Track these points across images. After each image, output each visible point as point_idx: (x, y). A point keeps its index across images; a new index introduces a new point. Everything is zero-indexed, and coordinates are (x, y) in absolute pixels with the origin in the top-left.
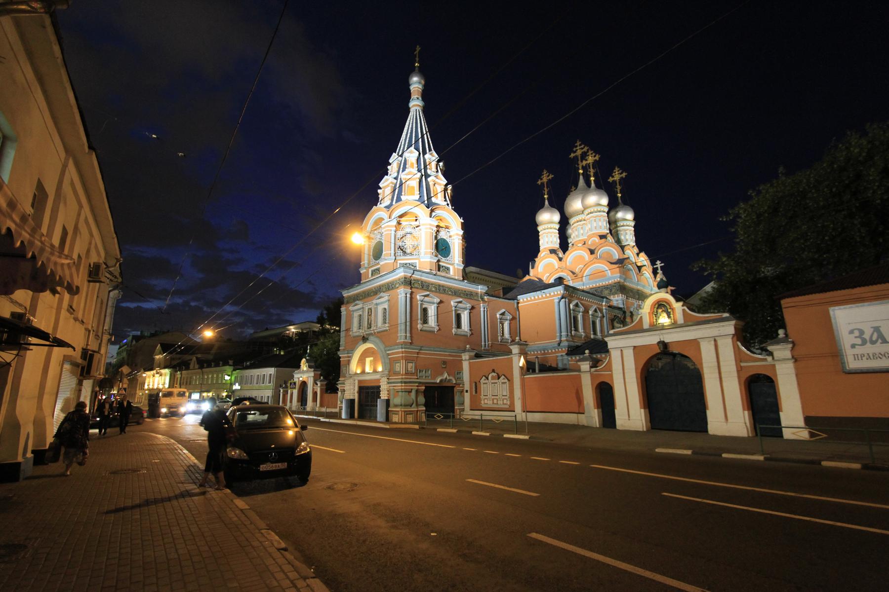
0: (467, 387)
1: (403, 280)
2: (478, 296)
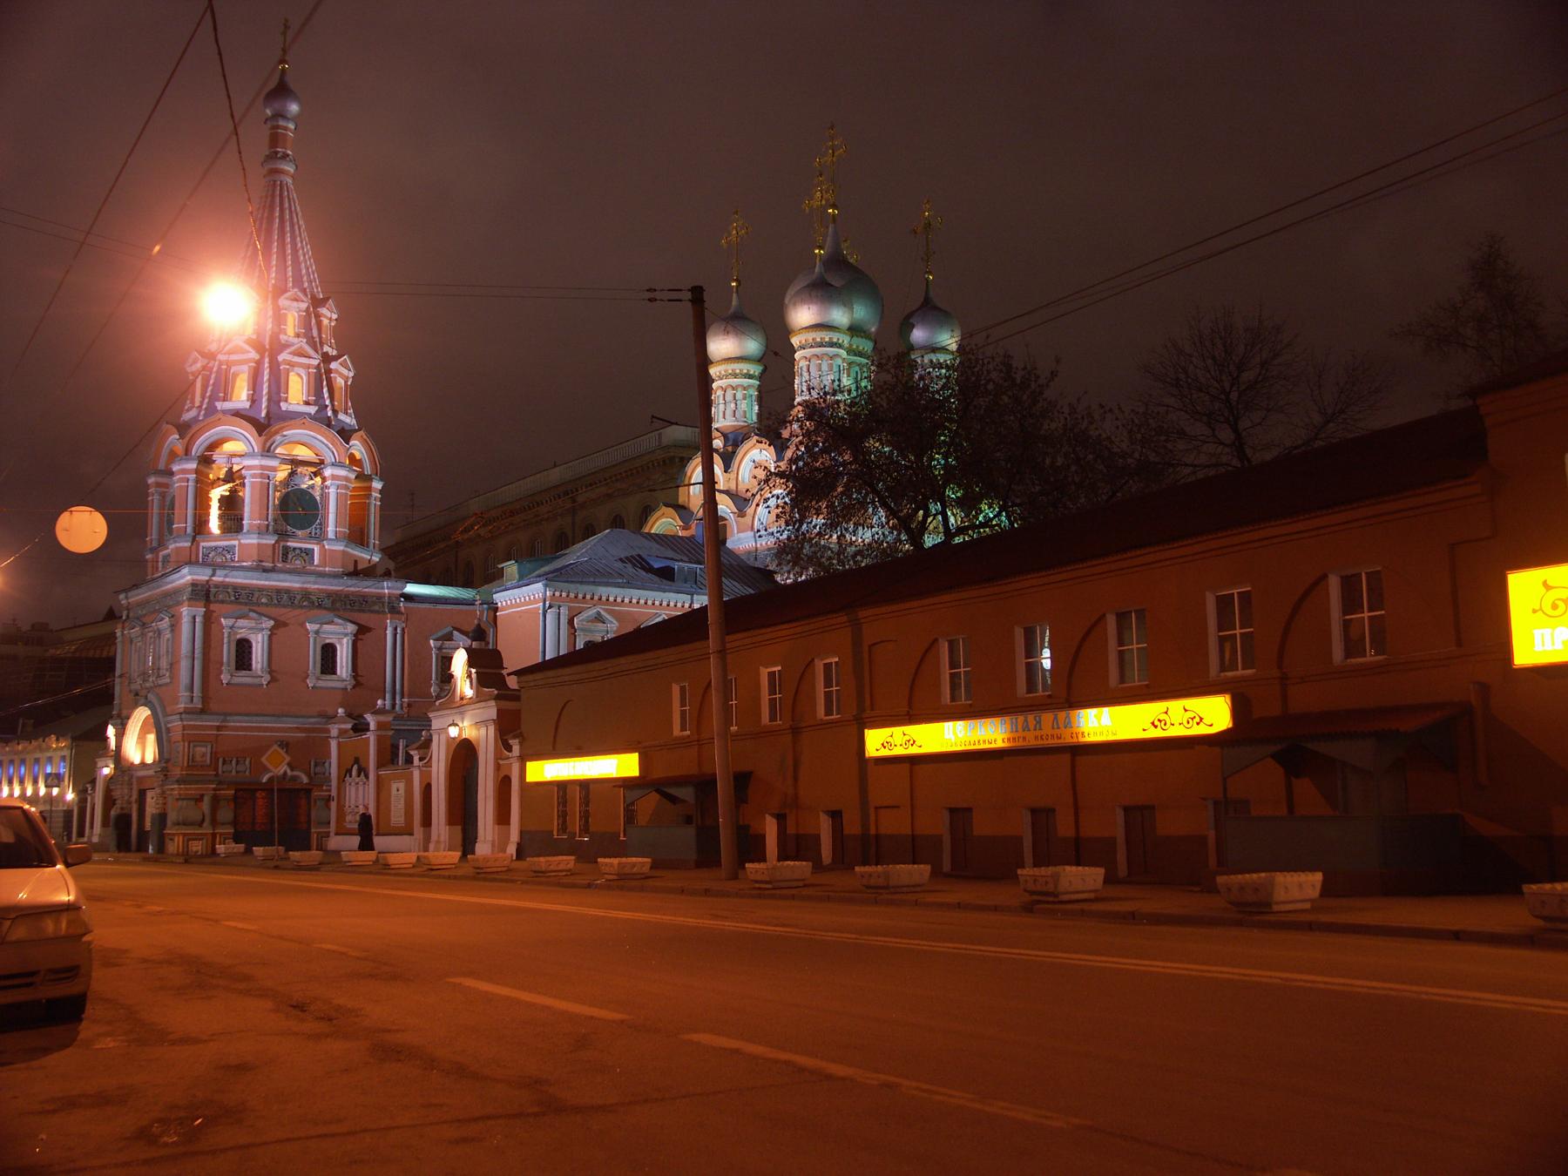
0: (334, 793)
1: (190, 589)
2: (383, 603)
